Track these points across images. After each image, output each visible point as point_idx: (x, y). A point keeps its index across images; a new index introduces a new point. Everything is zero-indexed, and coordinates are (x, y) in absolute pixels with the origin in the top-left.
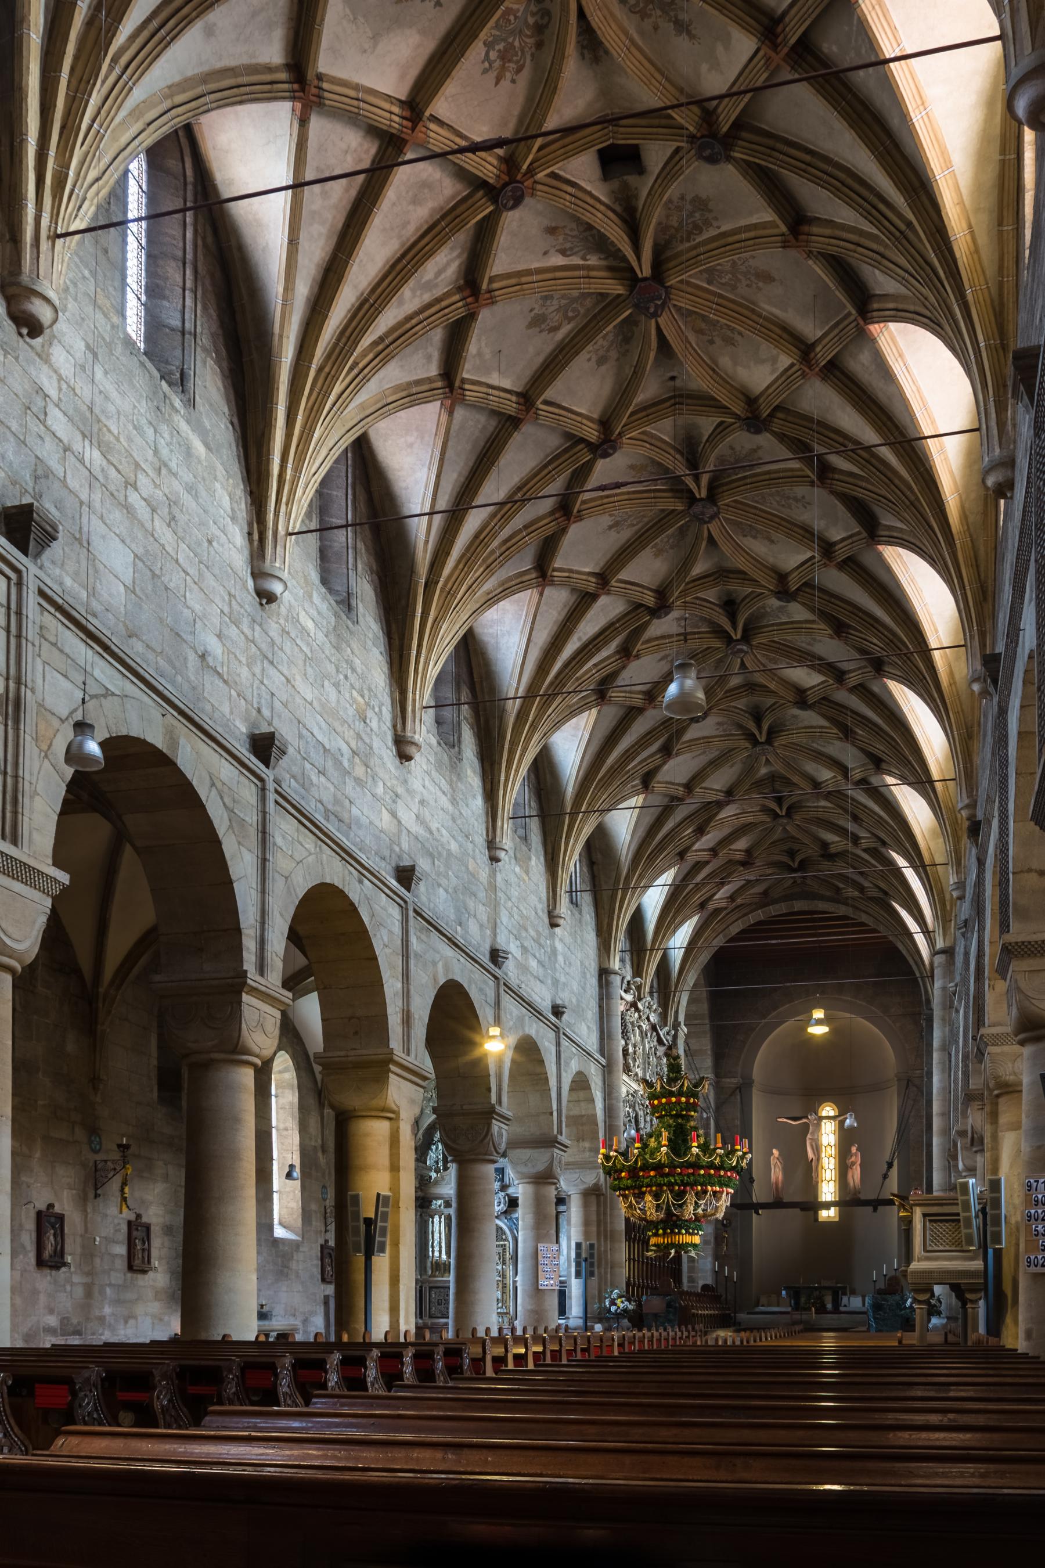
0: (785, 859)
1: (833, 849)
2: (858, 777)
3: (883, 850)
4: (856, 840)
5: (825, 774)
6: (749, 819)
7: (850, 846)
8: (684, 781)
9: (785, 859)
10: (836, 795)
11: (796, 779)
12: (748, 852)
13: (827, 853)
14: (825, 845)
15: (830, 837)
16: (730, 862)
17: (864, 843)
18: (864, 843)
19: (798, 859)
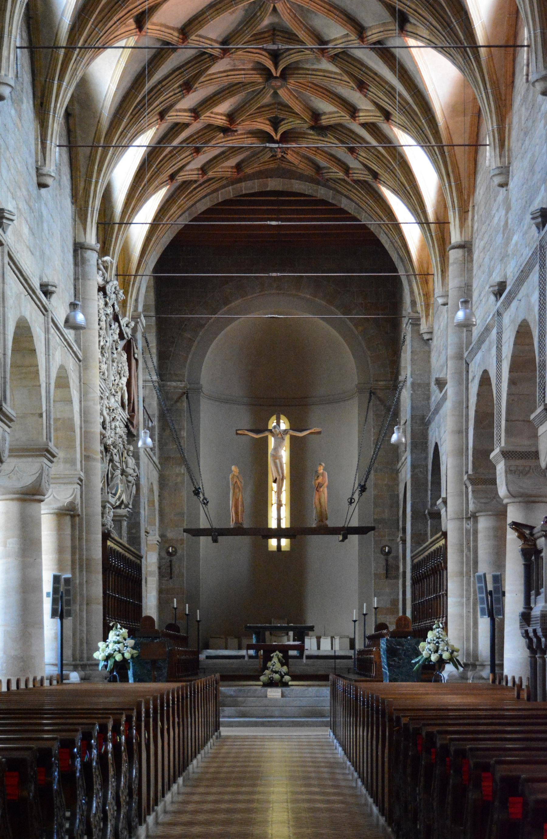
0: (268, 129)
1: (324, 121)
2: (375, 38)
3: (384, 126)
4: (353, 111)
5: (336, 32)
6: (241, 78)
7: (346, 120)
8: (179, 25)
9: (268, 129)
10: (342, 57)
11: (302, 35)
12: (231, 116)
13: (317, 125)
14: (316, 115)
15: (325, 107)
16: (210, 127)
17: (363, 117)
18: (363, 117)
19: (281, 130)
